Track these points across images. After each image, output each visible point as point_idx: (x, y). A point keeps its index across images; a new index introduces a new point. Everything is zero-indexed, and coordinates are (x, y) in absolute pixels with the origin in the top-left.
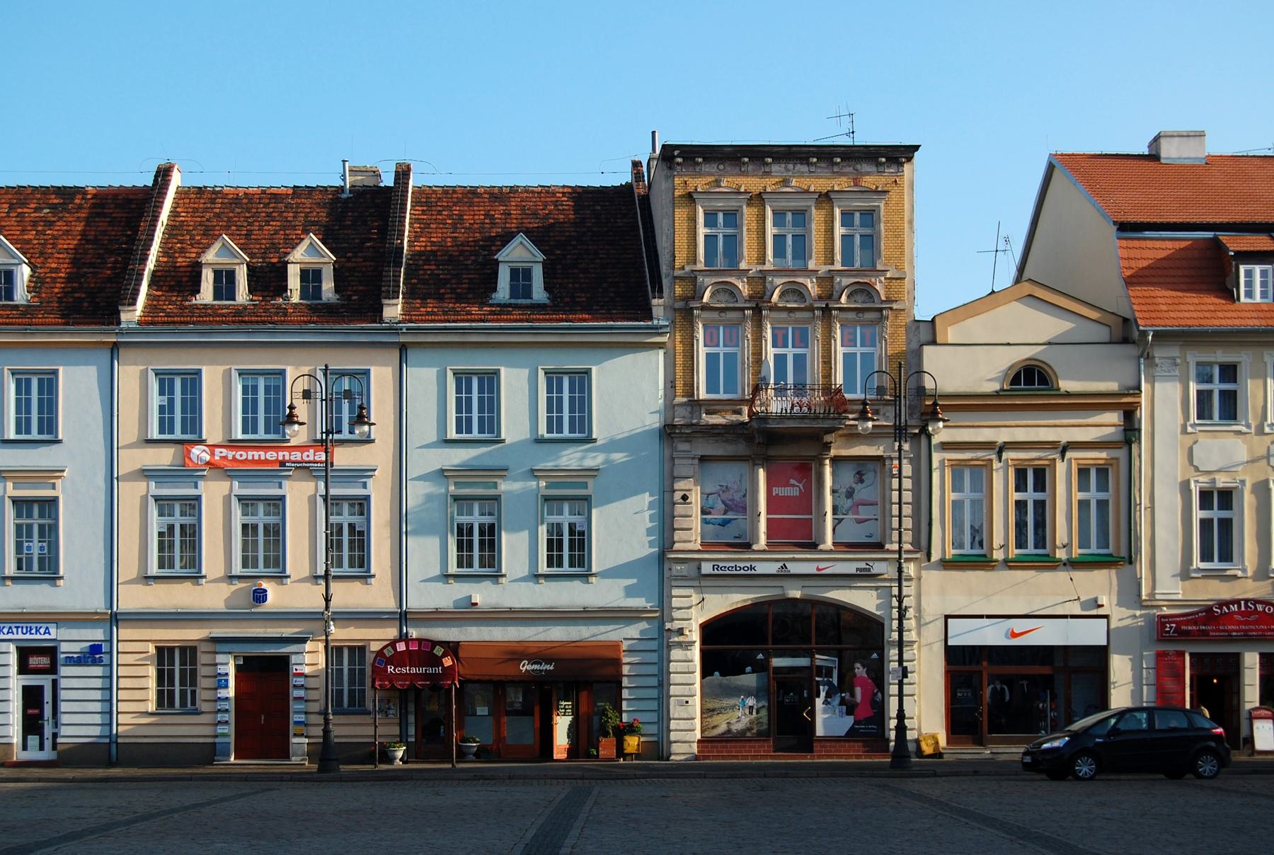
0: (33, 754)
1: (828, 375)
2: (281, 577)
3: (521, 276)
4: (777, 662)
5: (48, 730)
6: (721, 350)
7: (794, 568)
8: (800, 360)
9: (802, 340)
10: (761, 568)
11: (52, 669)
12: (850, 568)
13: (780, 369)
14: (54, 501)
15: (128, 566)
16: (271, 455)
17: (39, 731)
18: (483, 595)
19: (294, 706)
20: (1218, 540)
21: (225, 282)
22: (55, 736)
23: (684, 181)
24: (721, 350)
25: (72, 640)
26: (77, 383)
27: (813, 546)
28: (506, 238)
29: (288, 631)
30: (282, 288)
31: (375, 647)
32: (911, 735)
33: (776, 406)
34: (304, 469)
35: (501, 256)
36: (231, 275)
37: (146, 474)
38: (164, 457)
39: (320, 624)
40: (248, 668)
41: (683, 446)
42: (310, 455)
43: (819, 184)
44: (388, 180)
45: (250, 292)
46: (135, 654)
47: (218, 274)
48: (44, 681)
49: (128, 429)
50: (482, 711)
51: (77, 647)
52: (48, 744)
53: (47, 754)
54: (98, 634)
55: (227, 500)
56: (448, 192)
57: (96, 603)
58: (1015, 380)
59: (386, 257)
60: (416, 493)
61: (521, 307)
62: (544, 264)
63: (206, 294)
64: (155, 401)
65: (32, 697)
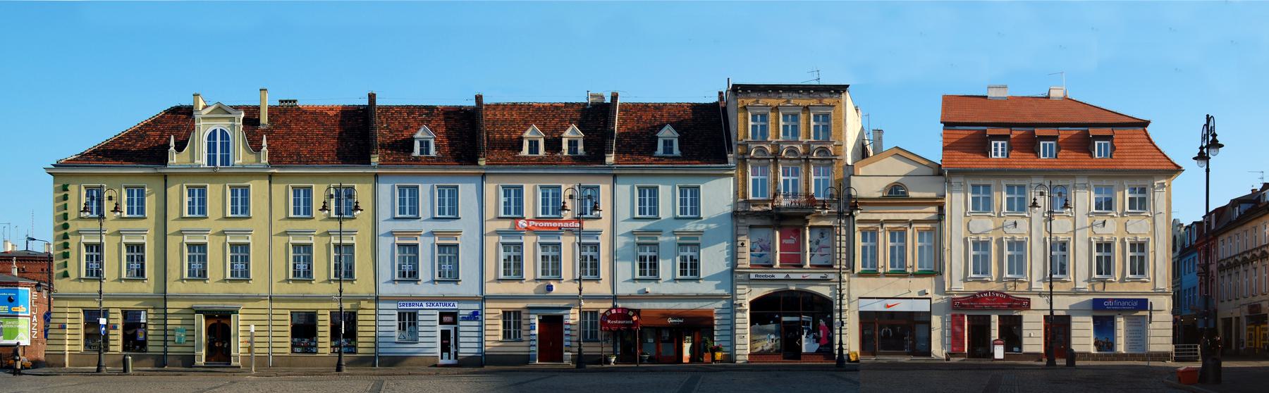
0: (445, 361)
1: (808, 189)
2: (559, 280)
3: (668, 144)
4: (784, 319)
5: (453, 350)
6: (759, 177)
7: (792, 276)
8: (795, 182)
9: (796, 173)
10: (778, 276)
11: (455, 322)
12: (818, 276)
13: (785, 187)
14: (457, 246)
15: (490, 274)
16: (555, 224)
17: (449, 351)
18: (651, 288)
19: (565, 338)
20: (981, 265)
21: (534, 146)
22: (456, 353)
23: (742, 101)
24: (759, 177)
25: (465, 309)
26: (467, 191)
27: (801, 266)
28: (662, 126)
29: (562, 304)
30: (560, 149)
31: (602, 311)
32: (845, 352)
33: (784, 203)
34: (570, 231)
35: (659, 135)
36: (537, 142)
37: (498, 233)
38: (506, 225)
39: (576, 302)
40: (545, 321)
41: (742, 221)
42: (572, 224)
43: (804, 102)
44: (608, 100)
45: (546, 150)
46: (493, 312)
47: (530, 142)
48: (451, 328)
49: (490, 212)
50: (651, 340)
51: (467, 313)
52: (452, 357)
53: (452, 361)
54: (476, 306)
55: (535, 245)
56: (635, 105)
57: (476, 292)
58: (891, 192)
59: (607, 135)
60: (621, 242)
61: (668, 158)
62: (679, 139)
63: (525, 151)
64: (502, 199)
65: (445, 335)
